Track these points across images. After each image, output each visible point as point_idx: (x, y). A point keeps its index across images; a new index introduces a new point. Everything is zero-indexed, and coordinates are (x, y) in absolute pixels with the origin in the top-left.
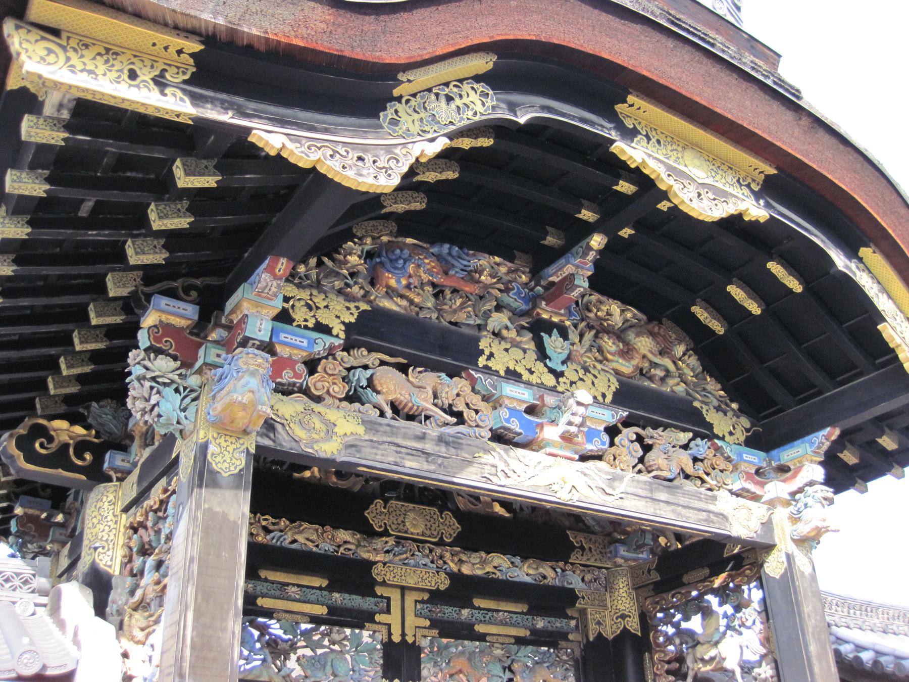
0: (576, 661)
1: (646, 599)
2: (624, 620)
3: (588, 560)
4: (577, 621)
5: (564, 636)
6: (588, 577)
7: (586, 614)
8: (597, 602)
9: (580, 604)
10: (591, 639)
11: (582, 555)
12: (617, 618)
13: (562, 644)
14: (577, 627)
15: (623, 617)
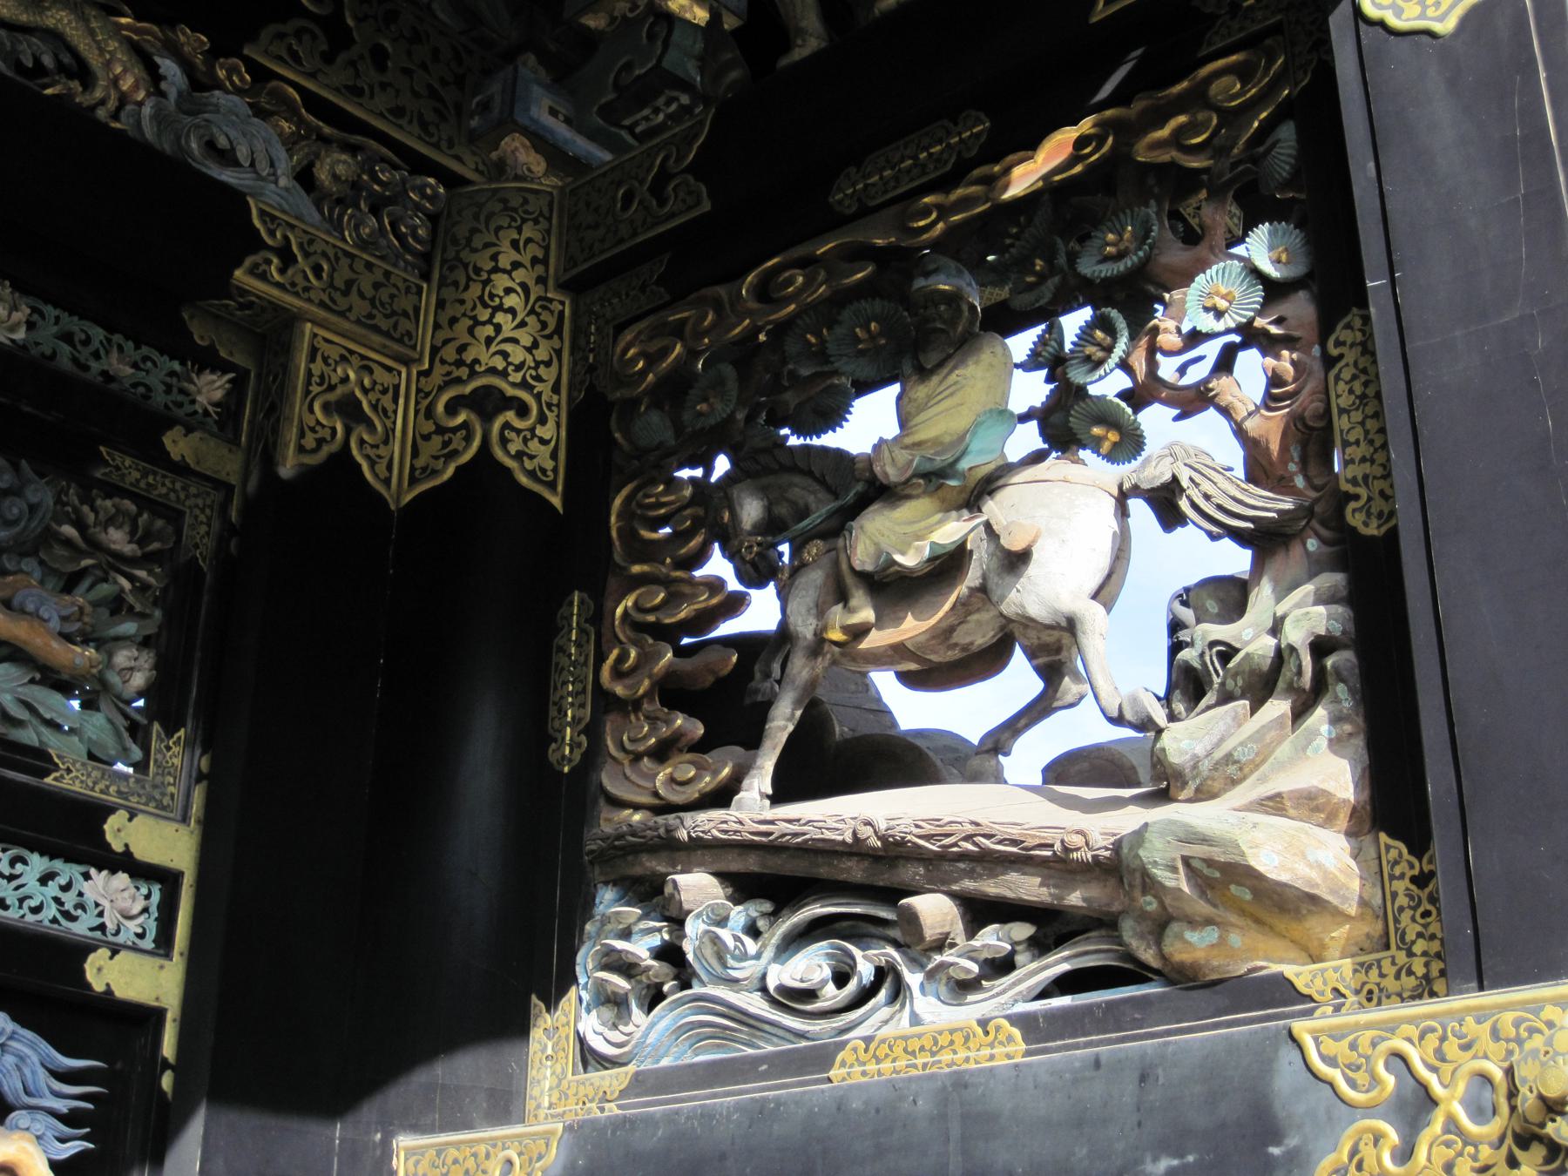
0: (184, 580)
1: (620, 329)
2: (487, 418)
3: (355, 92)
4: (238, 386)
5: (142, 428)
6: (334, 167)
7: (286, 349)
8: (360, 307)
9: (252, 272)
10: (286, 470)
11: (328, 58)
12: (451, 408)
13: (127, 468)
14: (229, 411)
15: (488, 403)
